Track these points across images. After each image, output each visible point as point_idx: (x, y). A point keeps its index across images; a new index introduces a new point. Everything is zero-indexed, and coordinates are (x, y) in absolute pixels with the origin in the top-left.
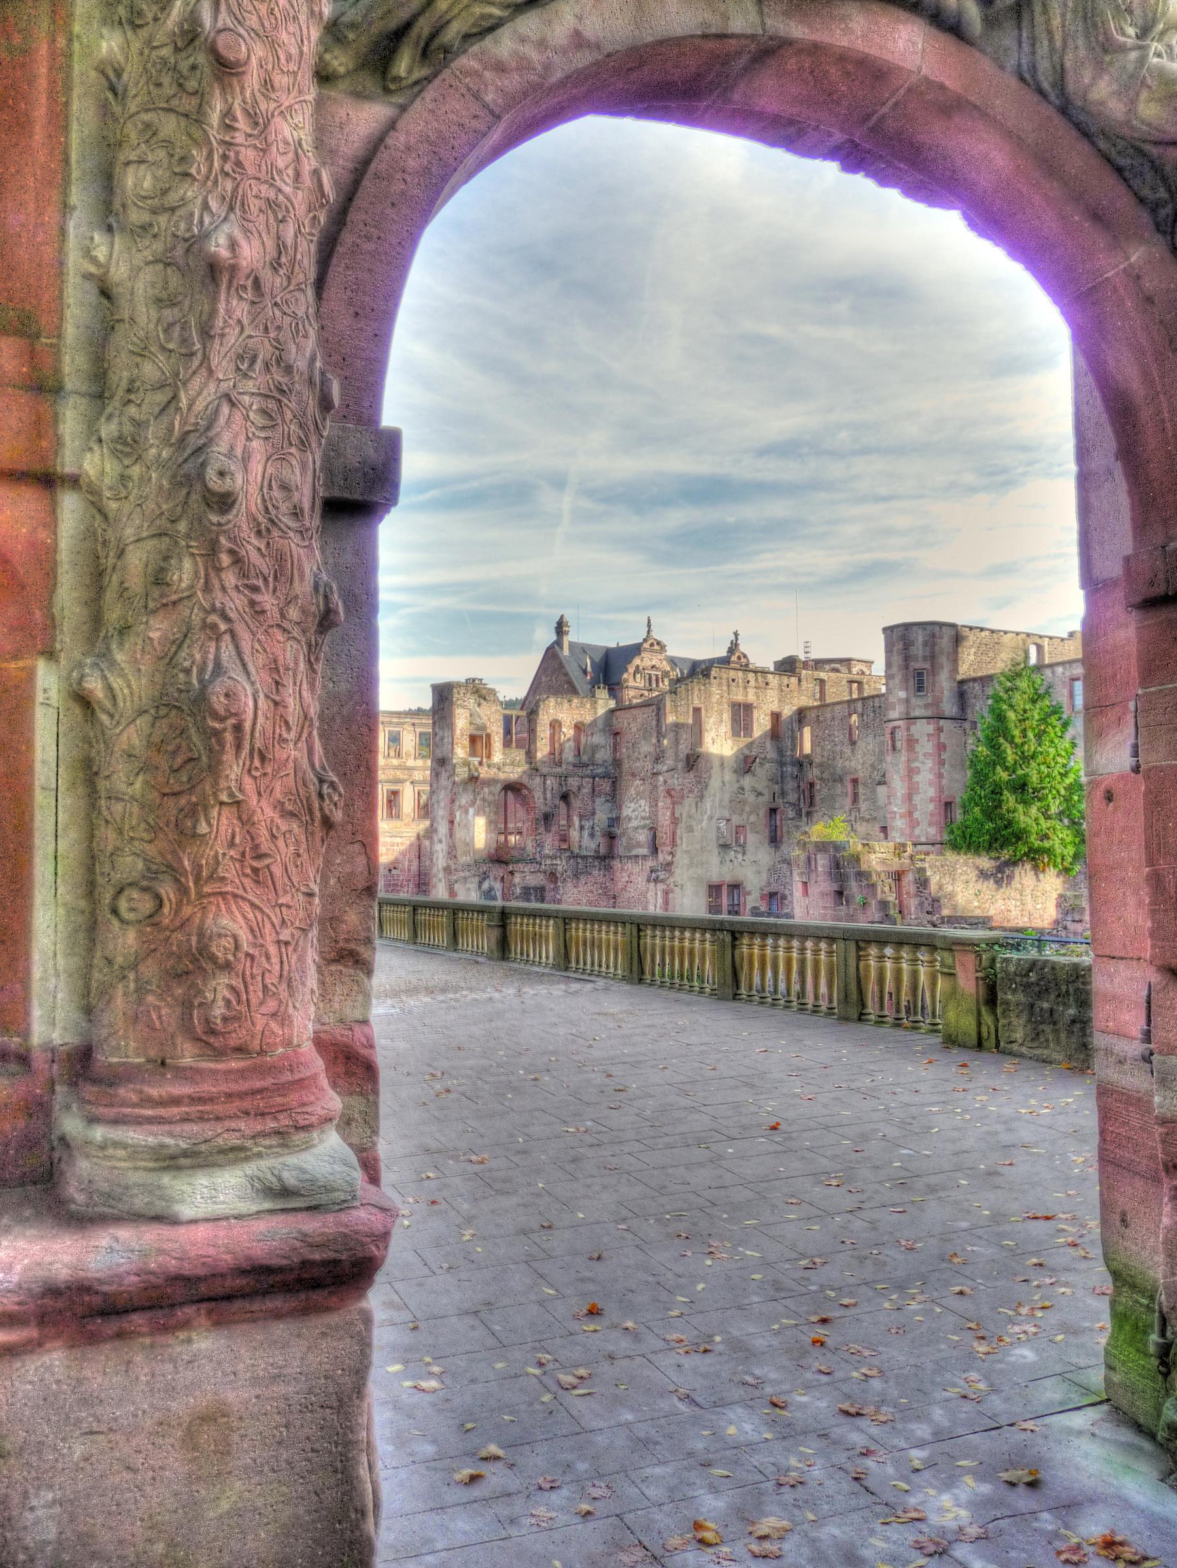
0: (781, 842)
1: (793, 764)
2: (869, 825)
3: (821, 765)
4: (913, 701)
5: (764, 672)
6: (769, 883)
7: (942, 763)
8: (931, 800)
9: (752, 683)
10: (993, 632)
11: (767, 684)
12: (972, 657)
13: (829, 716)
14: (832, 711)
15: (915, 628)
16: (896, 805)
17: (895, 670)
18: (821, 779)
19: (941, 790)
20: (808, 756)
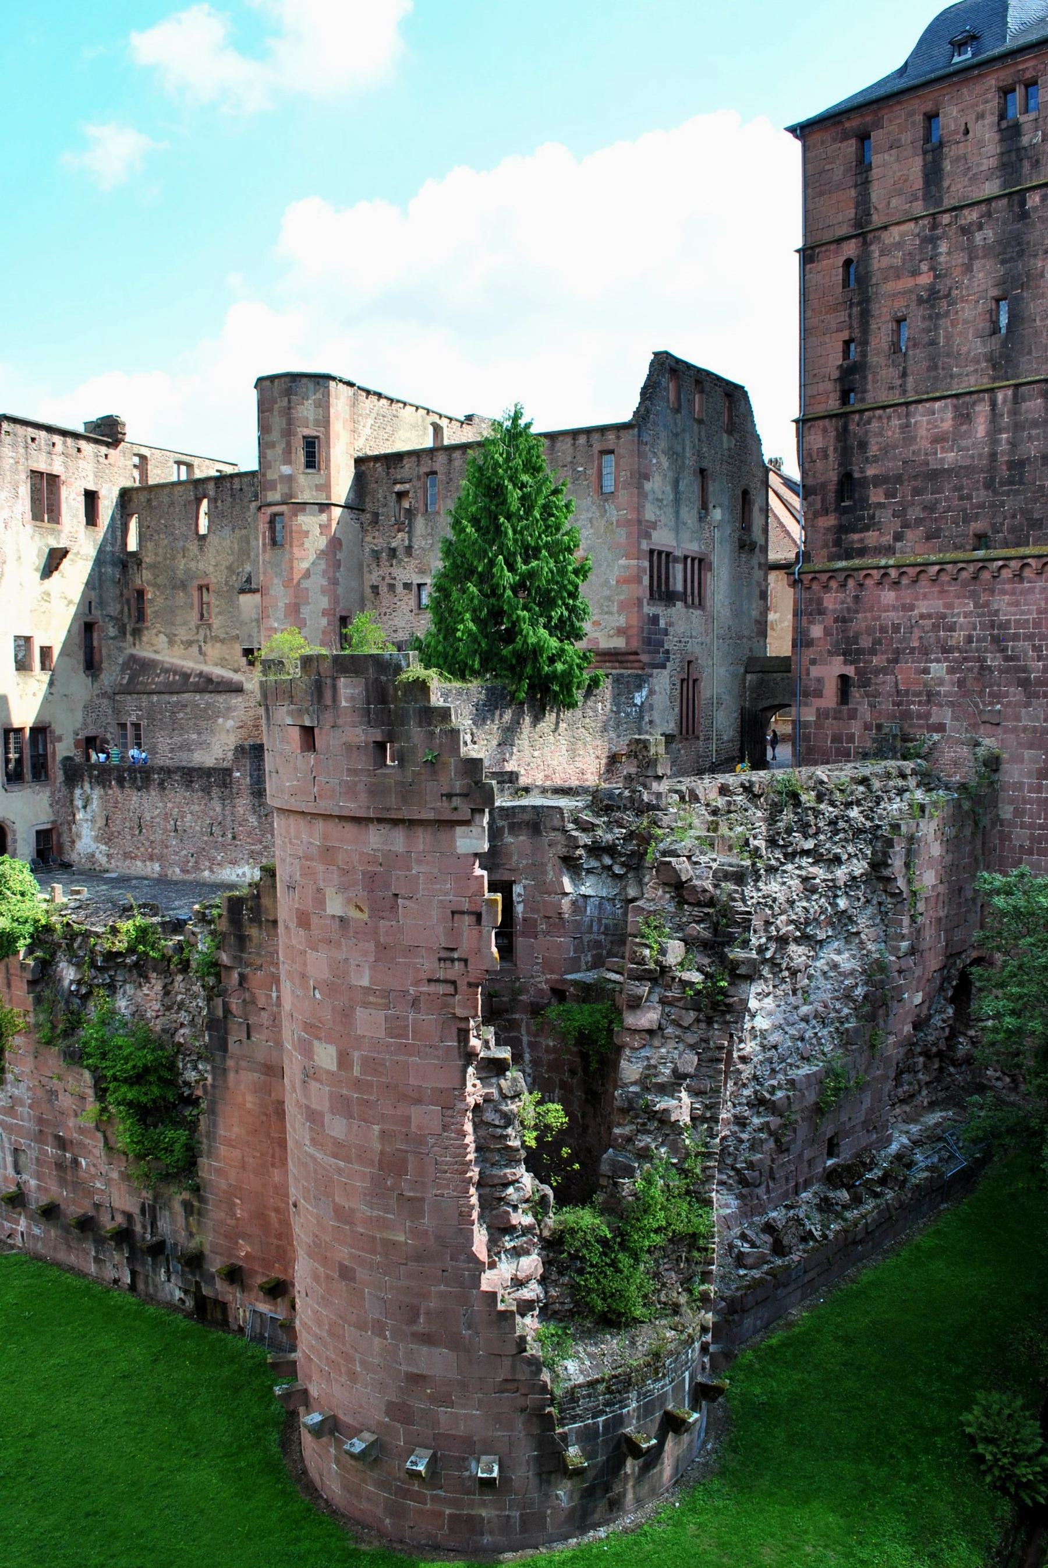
0: (100, 669)
1: (114, 565)
2: (224, 647)
3: (153, 566)
4: (302, 480)
5: (76, 436)
6: (85, 724)
7: (338, 565)
8: (324, 613)
9: (59, 447)
10: (391, 400)
11: (79, 450)
12: (368, 431)
13: (166, 500)
14: (171, 494)
15: (305, 380)
16: (277, 620)
17: (275, 435)
18: (155, 585)
19: (335, 600)
20: (132, 554)
